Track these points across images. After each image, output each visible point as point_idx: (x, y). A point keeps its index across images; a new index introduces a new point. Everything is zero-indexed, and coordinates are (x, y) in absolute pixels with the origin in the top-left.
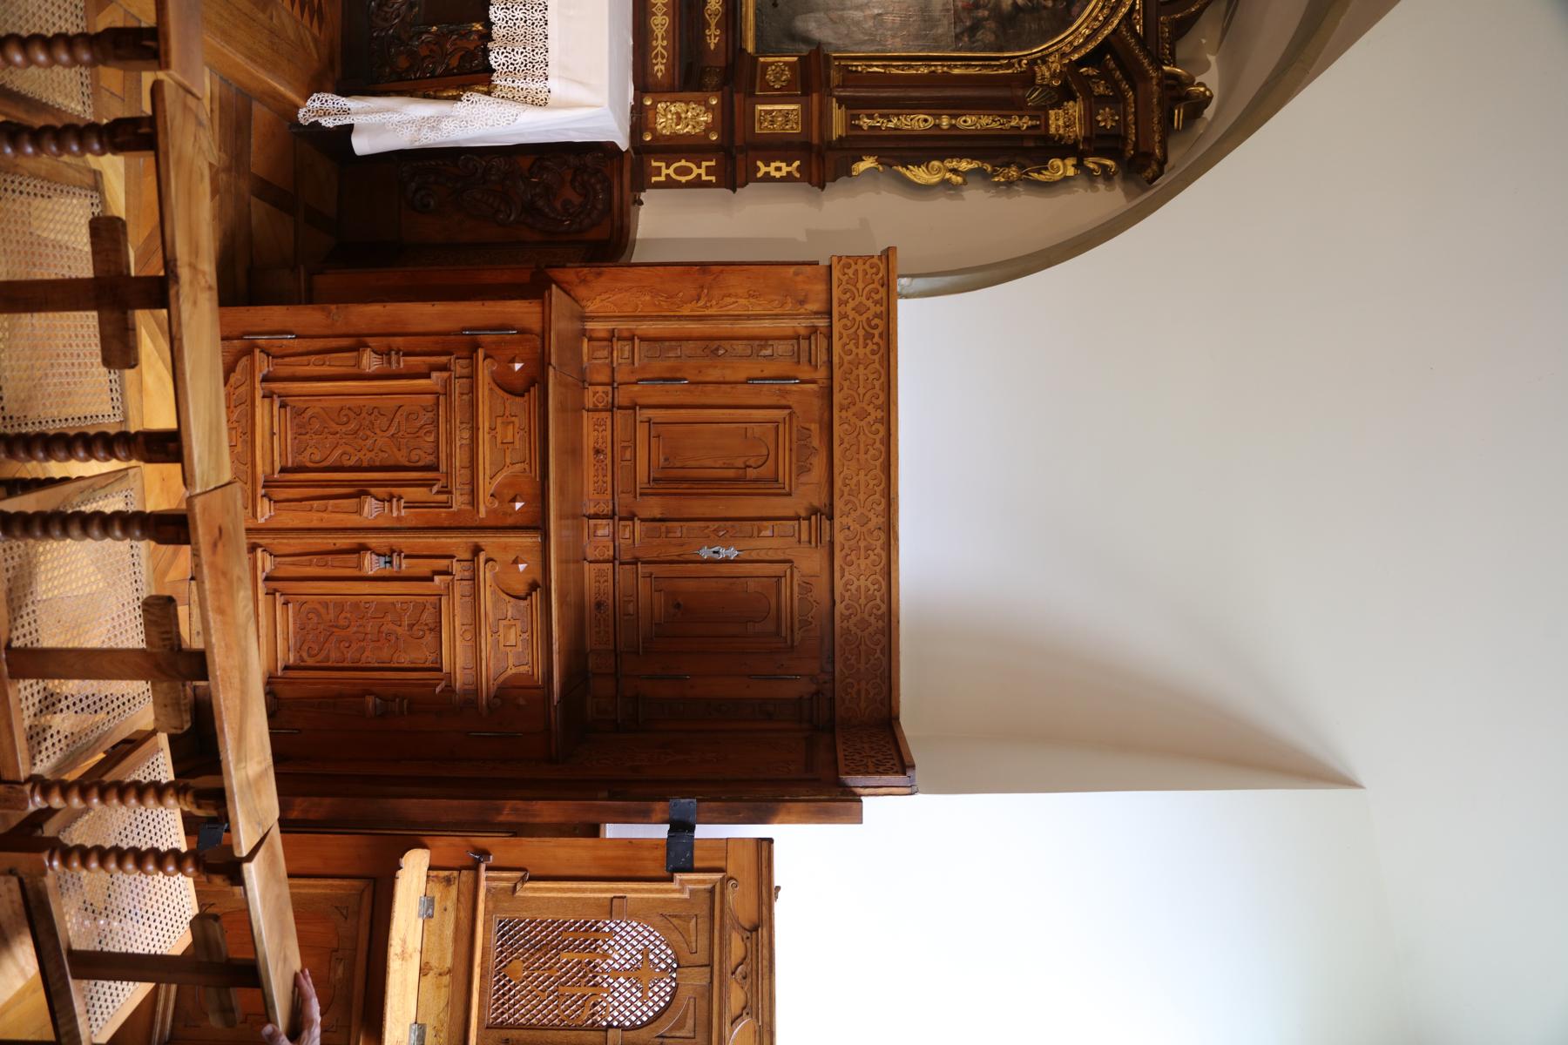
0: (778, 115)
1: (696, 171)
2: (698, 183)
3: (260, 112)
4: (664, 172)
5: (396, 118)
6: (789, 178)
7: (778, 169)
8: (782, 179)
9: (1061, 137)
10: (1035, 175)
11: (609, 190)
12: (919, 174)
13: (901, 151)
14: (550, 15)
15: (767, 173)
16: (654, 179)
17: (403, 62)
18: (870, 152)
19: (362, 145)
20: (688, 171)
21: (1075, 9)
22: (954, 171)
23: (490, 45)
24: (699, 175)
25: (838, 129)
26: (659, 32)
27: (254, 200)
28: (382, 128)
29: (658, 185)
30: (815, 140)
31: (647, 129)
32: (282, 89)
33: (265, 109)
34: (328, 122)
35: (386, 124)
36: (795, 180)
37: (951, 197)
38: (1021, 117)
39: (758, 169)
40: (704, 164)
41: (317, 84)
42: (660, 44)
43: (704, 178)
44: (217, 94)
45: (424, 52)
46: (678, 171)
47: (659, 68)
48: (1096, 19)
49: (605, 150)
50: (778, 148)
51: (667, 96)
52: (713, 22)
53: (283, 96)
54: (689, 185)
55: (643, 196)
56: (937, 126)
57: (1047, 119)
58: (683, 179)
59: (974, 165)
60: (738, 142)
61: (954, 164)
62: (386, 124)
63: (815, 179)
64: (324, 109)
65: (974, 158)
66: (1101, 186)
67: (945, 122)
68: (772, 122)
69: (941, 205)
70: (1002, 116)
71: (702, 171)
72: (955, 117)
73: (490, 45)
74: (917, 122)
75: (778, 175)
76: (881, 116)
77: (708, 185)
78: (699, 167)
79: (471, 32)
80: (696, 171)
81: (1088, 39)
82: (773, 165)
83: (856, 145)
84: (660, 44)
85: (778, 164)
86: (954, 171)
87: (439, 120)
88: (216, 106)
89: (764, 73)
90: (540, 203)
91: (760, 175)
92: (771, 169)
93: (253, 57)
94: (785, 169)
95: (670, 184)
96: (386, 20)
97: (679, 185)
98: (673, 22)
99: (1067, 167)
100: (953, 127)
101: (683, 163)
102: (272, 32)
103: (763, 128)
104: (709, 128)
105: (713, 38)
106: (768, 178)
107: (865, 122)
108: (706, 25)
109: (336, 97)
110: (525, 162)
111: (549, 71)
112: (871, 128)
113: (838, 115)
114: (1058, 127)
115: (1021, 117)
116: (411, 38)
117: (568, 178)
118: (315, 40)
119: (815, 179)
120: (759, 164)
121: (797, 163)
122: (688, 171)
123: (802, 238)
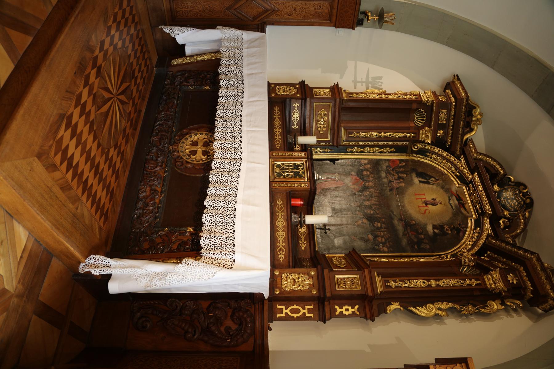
0: (348, 280)
1: (302, 311)
2: (303, 318)
3: (56, 265)
4: (284, 311)
5: (139, 271)
7: (347, 310)
9: (495, 289)
10: (483, 310)
11: (254, 322)
12: (422, 311)
13: (411, 300)
14: (237, 220)
15: (342, 312)
16: (278, 315)
17: (146, 246)
18: (396, 300)
19: (114, 288)
20: (298, 311)
21: (461, 234)
23: (201, 234)
24: (304, 314)
25: (380, 289)
27: (34, 317)
28: (129, 278)
29: (281, 319)
30: (370, 294)
31: (277, 288)
32: (72, 249)
33: (60, 263)
34: (96, 272)
35: (131, 276)
37: (438, 323)
38: (471, 280)
40: (307, 307)
41: (96, 250)
42: (281, 245)
43: (307, 315)
44: (29, 248)
45: (159, 240)
46: (293, 311)
47: (281, 256)
48: (472, 237)
49: (253, 298)
50: (349, 298)
51: (288, 270)
53: (72, 255)
54: (298, 319)
55: (271, 325)
56: (430, 286)
58: (295, 316)
59: (450, 305)
60: (328, 295)
61: (439, 305)
62: (131, 276)
63: (368, 315)
64: (97, 265)
65: (449, 302)
66: (514, 315)
67: (433, 283)
68: (345, 284)
69: (434, 328)
71: (306, 311)
72: (438, 280)
73: (201, 234)
74: (420, 283)
75: (347, 313)
76: (400, 281)
77: (309, 319)
78: (304, 309)
79: (186, 232)
80: (302, 311)
81: (473, 246)
82: (344, 308)
85: (347, 307)
86: (440, 309)
87: (165, 275)
88: (26, 255)
89: (332, 262)
90: (213, 328)
91: (337, 313)
93: (57, 225)
94: (351, 310)
95: (288, 318)
96: (141, 224)
97: (292, 319)
99: (495, 305)
100: (438, 285)
101: (295, 307)
102: (74, 215)
103: (341, 288)
104: (312, 287)
105: (303, 245)
106: (341, 315)
107: (392, 284)
109: (104, 258)
110: (205, 304)
111: (235, 249)
112: (396, 286)
113: (378, 280)
114: (490, 284)
116: (153, 234)
117: (230, 314)
118: (100, 228)
119: (368, 315)
120: (337, 307)
121: (357, 307)
122: (298, 311)
123: (368, 350)
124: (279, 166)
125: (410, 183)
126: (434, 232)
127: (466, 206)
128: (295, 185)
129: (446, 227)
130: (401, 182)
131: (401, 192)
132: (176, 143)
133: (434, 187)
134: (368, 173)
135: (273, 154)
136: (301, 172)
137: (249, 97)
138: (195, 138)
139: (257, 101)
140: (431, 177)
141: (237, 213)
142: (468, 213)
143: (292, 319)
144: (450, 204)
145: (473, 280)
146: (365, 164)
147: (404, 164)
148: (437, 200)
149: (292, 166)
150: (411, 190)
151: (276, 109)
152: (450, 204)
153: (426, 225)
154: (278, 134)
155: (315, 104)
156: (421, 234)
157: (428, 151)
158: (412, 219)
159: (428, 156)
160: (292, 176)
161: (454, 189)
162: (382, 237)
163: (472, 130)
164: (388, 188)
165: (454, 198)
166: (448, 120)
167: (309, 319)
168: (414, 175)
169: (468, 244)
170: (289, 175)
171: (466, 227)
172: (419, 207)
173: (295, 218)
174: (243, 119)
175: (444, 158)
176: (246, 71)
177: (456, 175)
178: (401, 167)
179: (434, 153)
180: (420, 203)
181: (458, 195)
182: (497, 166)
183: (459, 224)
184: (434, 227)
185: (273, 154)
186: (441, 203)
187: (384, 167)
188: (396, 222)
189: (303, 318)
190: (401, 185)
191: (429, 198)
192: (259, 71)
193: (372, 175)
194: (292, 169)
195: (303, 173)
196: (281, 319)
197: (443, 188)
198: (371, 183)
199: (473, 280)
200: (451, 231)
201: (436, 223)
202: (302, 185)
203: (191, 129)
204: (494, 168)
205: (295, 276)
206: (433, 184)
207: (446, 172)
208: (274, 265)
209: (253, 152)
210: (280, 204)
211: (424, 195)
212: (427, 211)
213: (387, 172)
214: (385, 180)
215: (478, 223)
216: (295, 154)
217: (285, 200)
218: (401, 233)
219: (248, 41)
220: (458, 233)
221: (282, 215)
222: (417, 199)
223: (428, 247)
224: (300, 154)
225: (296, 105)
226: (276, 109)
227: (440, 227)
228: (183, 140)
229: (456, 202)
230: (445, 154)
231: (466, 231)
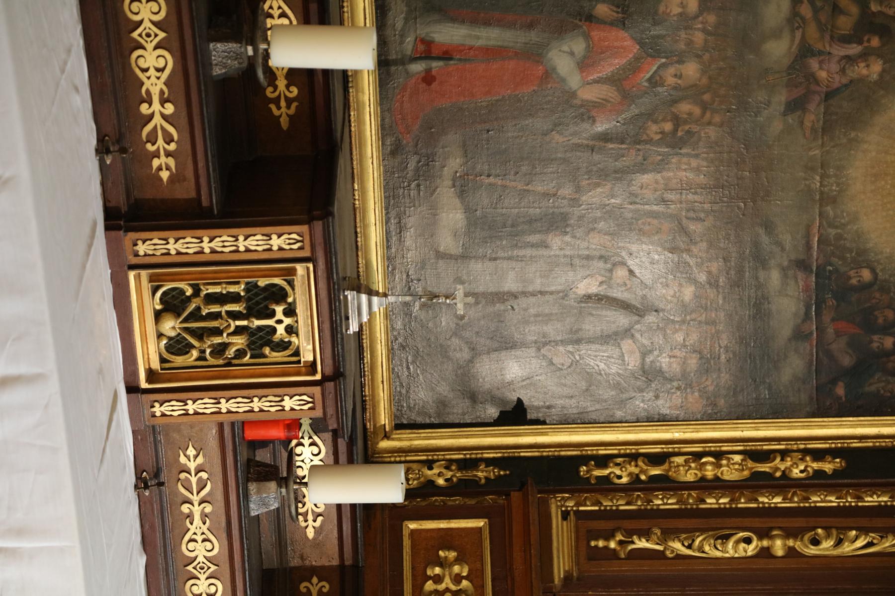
128: (256, 405)
130: (864, 56)
135: (142, 248)
136: (281, 329)
149: (234, 298)
154: (154, 85)
156: (886, 330)
158: (862, 258)
160: (240, 354)
170: (225, 346)
185: (142, 248)
190: (861, 69)
193: (711, 18)
195: (290, 330)
198: (691, 70)
202: (288, 403)
210: (192, 465)
216: (252, 243)
221: (204, 516)
224: (276, 242)
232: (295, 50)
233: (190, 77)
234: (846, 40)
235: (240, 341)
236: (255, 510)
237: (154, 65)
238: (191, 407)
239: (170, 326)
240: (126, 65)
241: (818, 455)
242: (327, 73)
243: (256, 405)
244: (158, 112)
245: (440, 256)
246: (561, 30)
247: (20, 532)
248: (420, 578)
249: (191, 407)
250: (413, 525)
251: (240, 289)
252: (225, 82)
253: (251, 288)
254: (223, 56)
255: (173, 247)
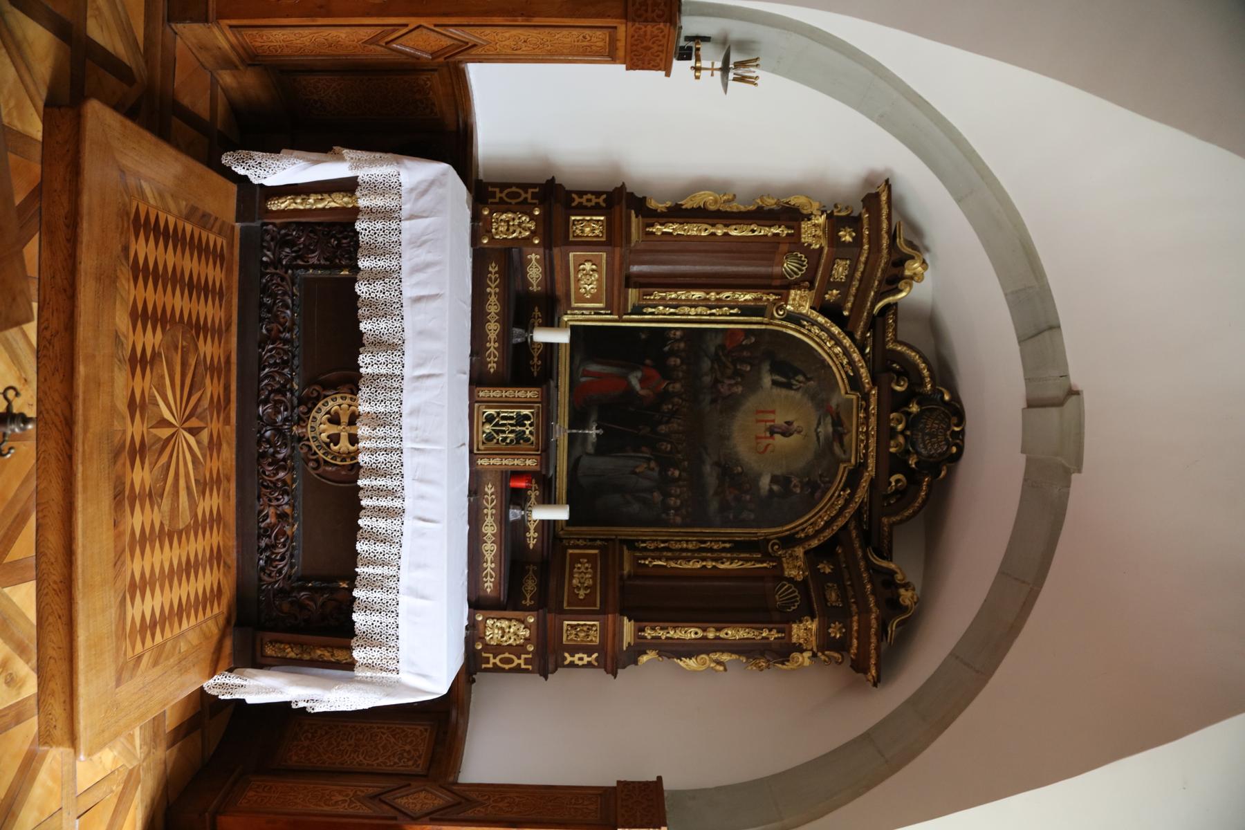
1: (517, 661)
2: (518, 670)
4: (492, 661)
6: (589, 665)
8: (583, 666)
12: (691, 663)
20: (510, 661)
21: (817, 494)
22: (719, 663)
26: (489, 557)
29: (487, 670)
36: (593, 666)
38: (770, 630)
39: (565, 659)
40: (523, 656)
42: (489, 566)
43: (523, 666)
46: (503, 661)
47: (489, 585)
51: (494, 613)
52: (532, 527)
57: (791, 631)
58: (507, 667)
67: (711, 635)
70: (757, 629)
71: (522, 662)
72: (718, 630)
75: (580, 663)
76: (662, 629)
77: (526, 671)
80: (517, 661)
81: (828, 524)
82: (577, 656)
83: (639, 648)
84: (489, 566)
91: (566, 662)
92: (576, 659)
94: (586, 659)
95: (496, 669)
97: (503, 670)
98: (500, 549)
106: (572, 665)
108: (528, 530)
112: (653, 638)
115: (770, 630)
119: (609, 669)
120: (566, 655)
121: (595, 655)
122: (511, 661)
124: (490, 419)
125: (753, 385)
126: (771, 490)
127: (846, 439)
128: (516, 462)
129: (795, 481)
130: (736, 384)
131: (731, 405)
132: (301, 421)
133: (798, 395)
134: (678, 361)
135: (481, 394)
137: (419, 365)
138: (332, 406)
139: (429, 376)
140: (797, 372)
141: (401, 609)
142: (845, 452)
143: (503, 670)
144: (817, 434)
145: (774, 631)
146: (677, 340)
147: (753, 340)
148: (795, 425)
149: (511, 418)
150: (751, 403)
151: (493, 268)
152: (817, 434)
153: (760, 475)
155: (571, 255)
157: (806, 317)
159: (804, 326)
160: (512, 441)
161: (833, 403)
162: (677, 497)
163: (901, 291)
164: (708, 398)
165: (829, 420)
166: (850, 277)
167: (526, 671)
168: (766, 367)
169: (817, 521)
171: (831, 482)
172: (757, 438)
173: (515, 514)
174: (405, 421)
175: (832, 336)
176: (410, 290)
177: (846, 373)
178: (746, 347)
179: (814, 323)
180: (761, 429)
181: (838, 414)
182: (926, 372)
183: (821, 476)
184: (774, 479)
185: (481, 394)
186: (799, 432)
187: (712, 349)
188: (707, 468)
189: (518, 670)
191: (780, 420)
192: (433, 292)
193: (684, 367)
194: (512, 425)
196: (487, 670)
197: (813, 397)
198: (678, 386)
199: (774, 631)
200: (802, 489)
201: (778, 472)
202: (528, 462)
203: (324, 389)
204: (919, 372)
205: (505, 624)
206: (797, 390)
207: (831, 363)
208: (477, 603)
209: (422, 497)
211: (773, 412)
212: (770, 448)
213: (716, 359)
214: (707, 379)
215: (853, 481)
217: (498, 484)
218: (711, 492)
219: (412, 190)
220: (812, 493)
222: (758, 421)
223: (752, 516)
224: (529, 394)
225: (533, 256)
226: (493, 268)
227: (782, 480)
228: (313, 413)
229: (830, 429)
230: (835, 330)
231: (828, 489)
232: (542, 336)
233: (504, 336)
234: (729, 378)
235: (512, 436)
236: (512, 518)
237: (493, 328)
238: (492, 462)
239: (488, 428)
240: (484, 309)
241: (724, 542)
242: (552, 344)
243: (516, 462)
244: (492, 346)
245: (588, 454)
246: (634, 369)
247: (426, 441)
248: (572, 568)
249: (492, 462)
250: (570, 551)
251: (514, 415)
252: (518, 345)
253: (518, 414)
254: (517, 335)
255: (492, 394)
